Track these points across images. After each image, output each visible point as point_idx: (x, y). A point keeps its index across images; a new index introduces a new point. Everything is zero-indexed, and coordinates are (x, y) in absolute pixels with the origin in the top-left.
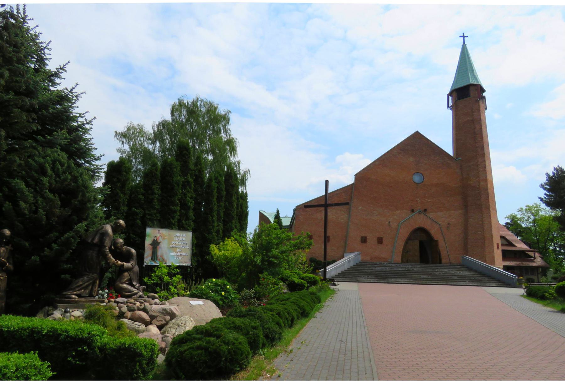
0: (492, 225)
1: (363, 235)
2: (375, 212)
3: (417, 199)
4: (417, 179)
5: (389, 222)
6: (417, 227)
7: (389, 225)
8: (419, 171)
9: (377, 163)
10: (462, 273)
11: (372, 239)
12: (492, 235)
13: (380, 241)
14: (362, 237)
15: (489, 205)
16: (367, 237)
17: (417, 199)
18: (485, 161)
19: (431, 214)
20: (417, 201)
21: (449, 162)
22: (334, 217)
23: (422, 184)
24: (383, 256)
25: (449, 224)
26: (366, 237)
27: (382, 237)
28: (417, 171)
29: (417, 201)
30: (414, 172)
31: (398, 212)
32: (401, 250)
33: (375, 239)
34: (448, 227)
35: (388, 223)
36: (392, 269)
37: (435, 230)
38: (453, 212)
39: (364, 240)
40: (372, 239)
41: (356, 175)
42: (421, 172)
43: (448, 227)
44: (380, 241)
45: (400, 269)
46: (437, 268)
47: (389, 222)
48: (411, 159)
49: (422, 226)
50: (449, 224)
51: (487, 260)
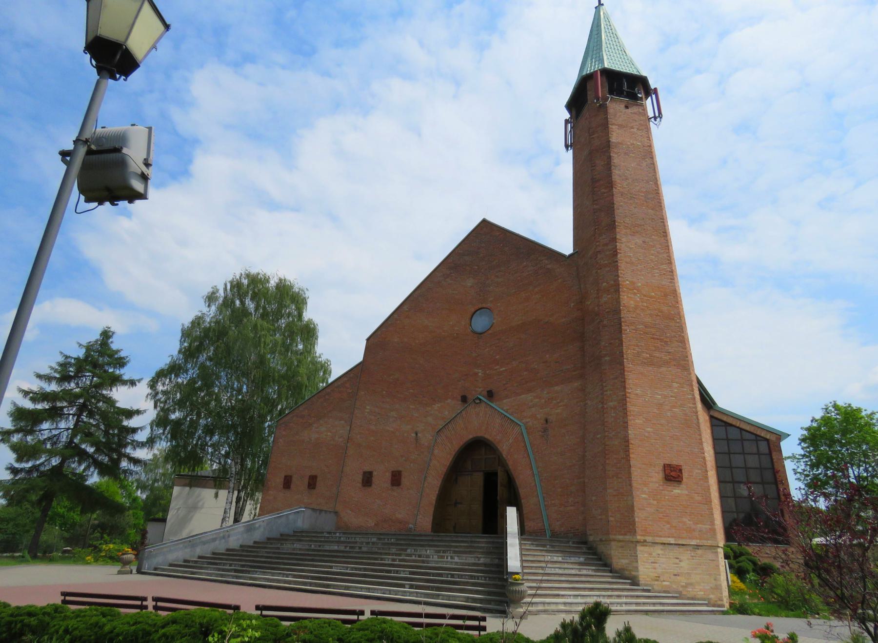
0: (630, 407)
1: (367, 469)
2: (393, 414)
3: (476, 370)
4: (480, 323)
5: (417, 434)
6: (471, 437)
7: (417, 439)
8: (484, 305)
9: (405, 307)
10: (456, 559)
11: (382, 479)
12: (626, 441)
13: (396, 479)
14: (365, 473)
15: (622, 353)
16: (375, 473)
17: (476, 370)
18: (614, 240)
19: (505, 401)
20: (476, 374)
21: (549, 266)
22: (329, 434)
23: (490, 332)
24: (399, 516)
25: (547, 421)
26: (371, 473)
27: (400, 469)
28: (480, 306)
29: (476, 374)
30: (473, 310)
31: (437, 406)
32: (433, 498)
33: (388, 475)
34: (545, 430)
35: (414, 435)
36: (321, 548)
37: (511, 441)
38: (556, 388)
39: (367, 479)
40: (382, 479)
41: (368, 340)
42: (489, 305)
43: (545, 430)
44: (396, 479)
45: (336, 548)
46: (409, 545)
47: (417, 434)
48: (470, 282)
49: (480, 434)
50: (547, 421)
51: (611, 519)
